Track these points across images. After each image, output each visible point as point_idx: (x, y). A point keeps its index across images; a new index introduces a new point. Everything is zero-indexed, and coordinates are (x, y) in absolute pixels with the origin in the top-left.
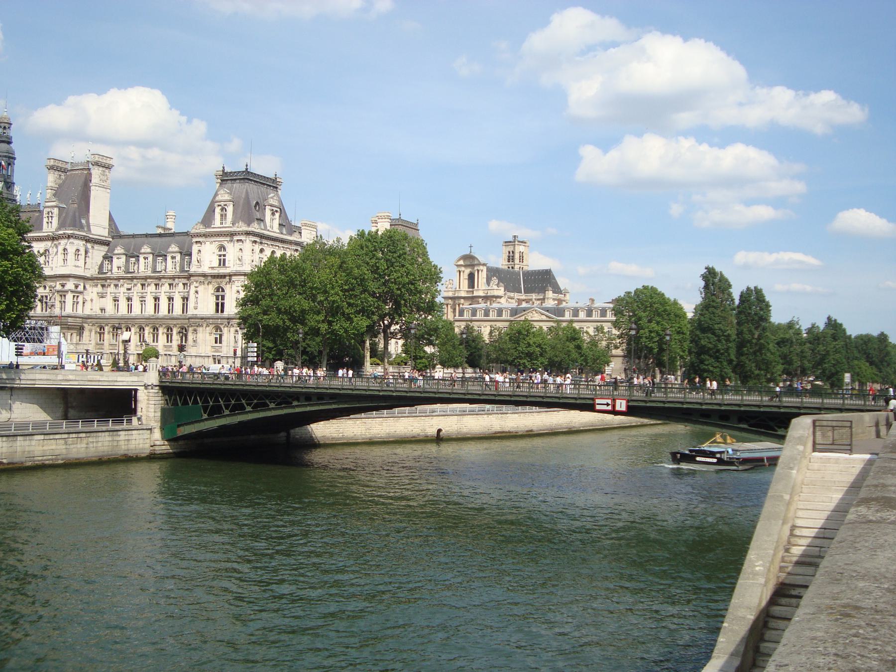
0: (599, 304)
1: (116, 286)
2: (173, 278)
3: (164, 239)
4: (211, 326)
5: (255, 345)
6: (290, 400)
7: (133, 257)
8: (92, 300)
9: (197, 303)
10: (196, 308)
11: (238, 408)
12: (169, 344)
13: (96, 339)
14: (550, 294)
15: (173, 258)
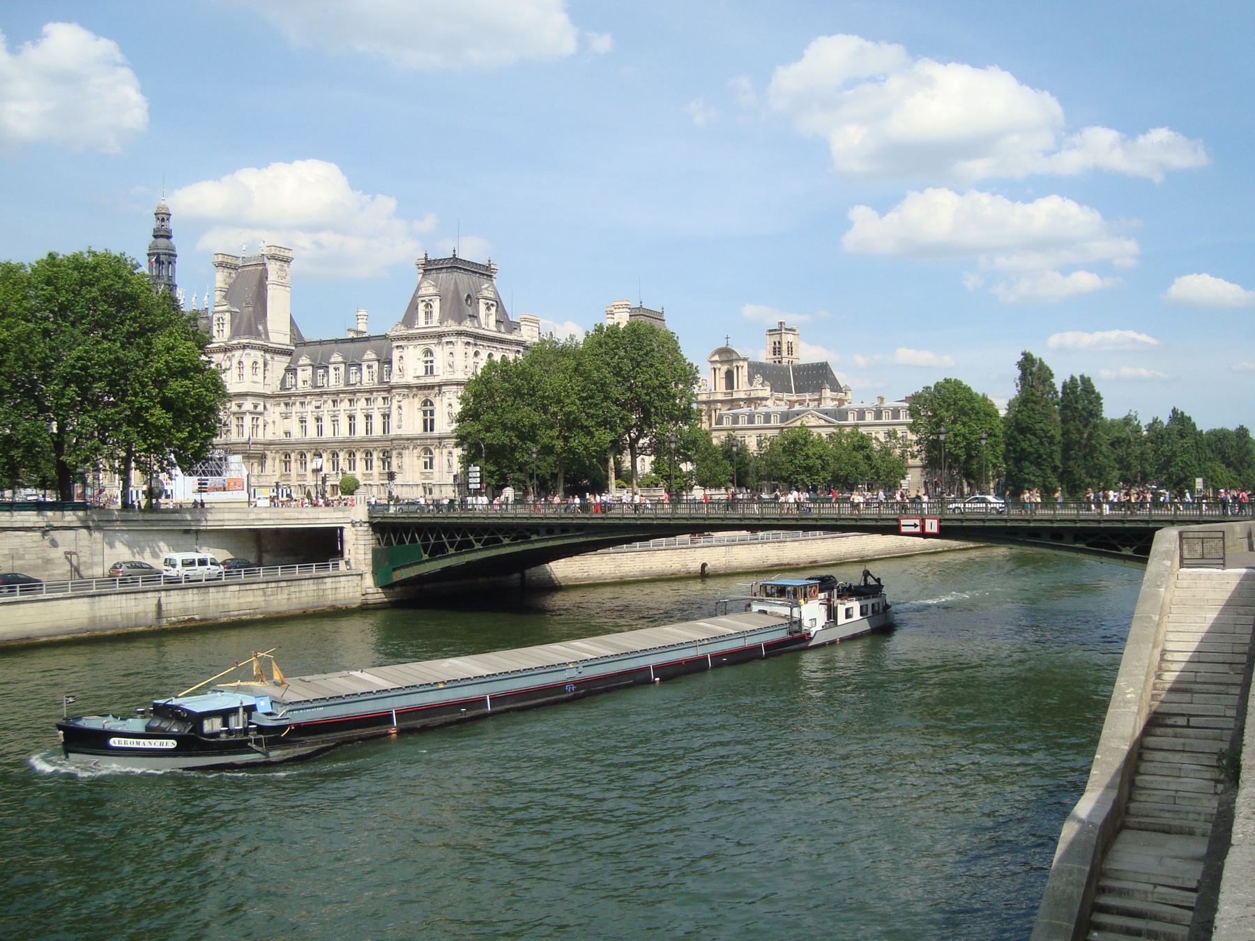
0: (889, 403)
1: (302, 403)
2: (371, 391)
3: (357, 345)
4: (419, 449)
5: (478, 469)
6: (528, 534)
7: (320, 368)
8: (274, 422)
9: (400, 420)
10: (399, 427)
11: (466, 546)
12: (369, 471)
13: (281, 469)
14: (827, 393)
15: (369, 367)
